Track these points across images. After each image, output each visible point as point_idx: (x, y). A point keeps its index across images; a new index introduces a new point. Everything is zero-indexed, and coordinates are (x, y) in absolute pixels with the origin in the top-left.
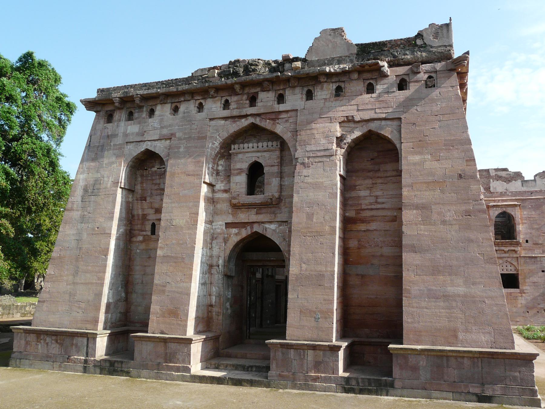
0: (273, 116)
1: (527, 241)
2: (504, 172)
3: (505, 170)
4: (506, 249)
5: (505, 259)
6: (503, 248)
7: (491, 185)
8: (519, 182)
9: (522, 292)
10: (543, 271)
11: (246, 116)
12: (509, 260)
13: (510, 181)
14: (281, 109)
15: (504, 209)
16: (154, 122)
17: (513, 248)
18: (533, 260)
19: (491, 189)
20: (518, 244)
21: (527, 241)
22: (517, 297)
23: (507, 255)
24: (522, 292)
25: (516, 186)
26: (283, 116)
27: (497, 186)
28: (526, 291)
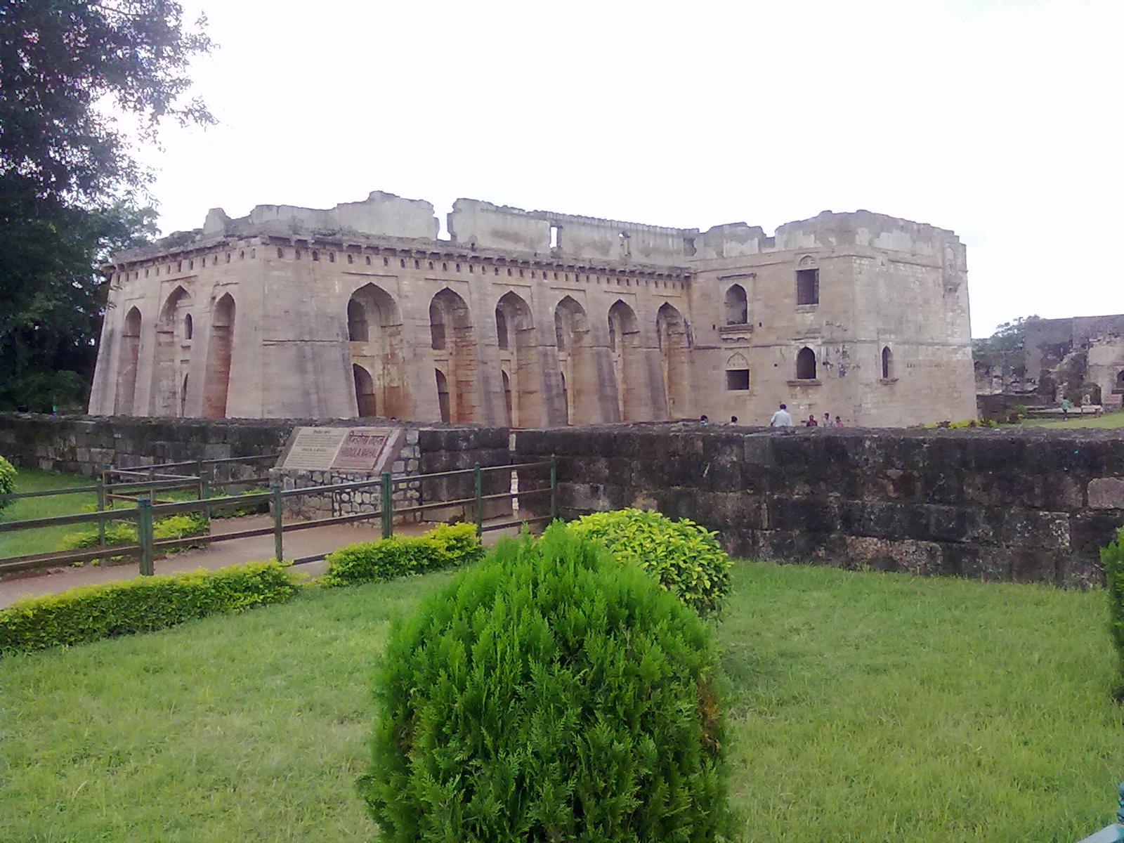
0: (189, 280)
1: (760, 325)
2: (739, 228)
3: (744, 224)
4: (735, 337)
5: (737, 350)
6: (730, 336)
7: (724, 248)
8: (756, 240)
9: (752, 394)
10: (776, 365)
11: (176, 280)
12: (740, 351)
13: (746, 241)
14: (192, 275)
15: (735, 282)
16: (137, 284)
17: (741, 336)
18: (765, 349)
19: (724, 254)
20: (751, 329)
21: (760, 325)
22: (746, 400)
23: (737, 345)
24: (752, 394)
25: (752, 246)
26: (193, 279)
27: (732, 249)
28: (755, 393)
